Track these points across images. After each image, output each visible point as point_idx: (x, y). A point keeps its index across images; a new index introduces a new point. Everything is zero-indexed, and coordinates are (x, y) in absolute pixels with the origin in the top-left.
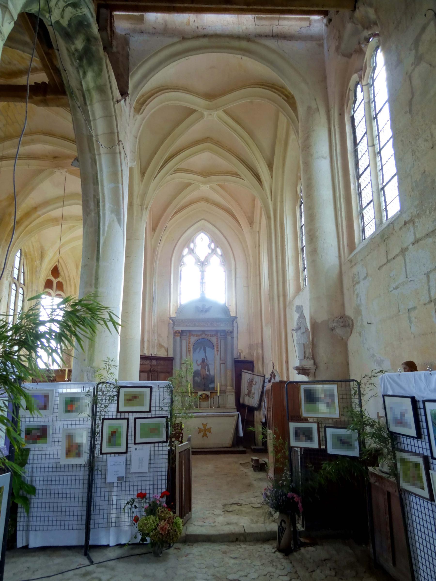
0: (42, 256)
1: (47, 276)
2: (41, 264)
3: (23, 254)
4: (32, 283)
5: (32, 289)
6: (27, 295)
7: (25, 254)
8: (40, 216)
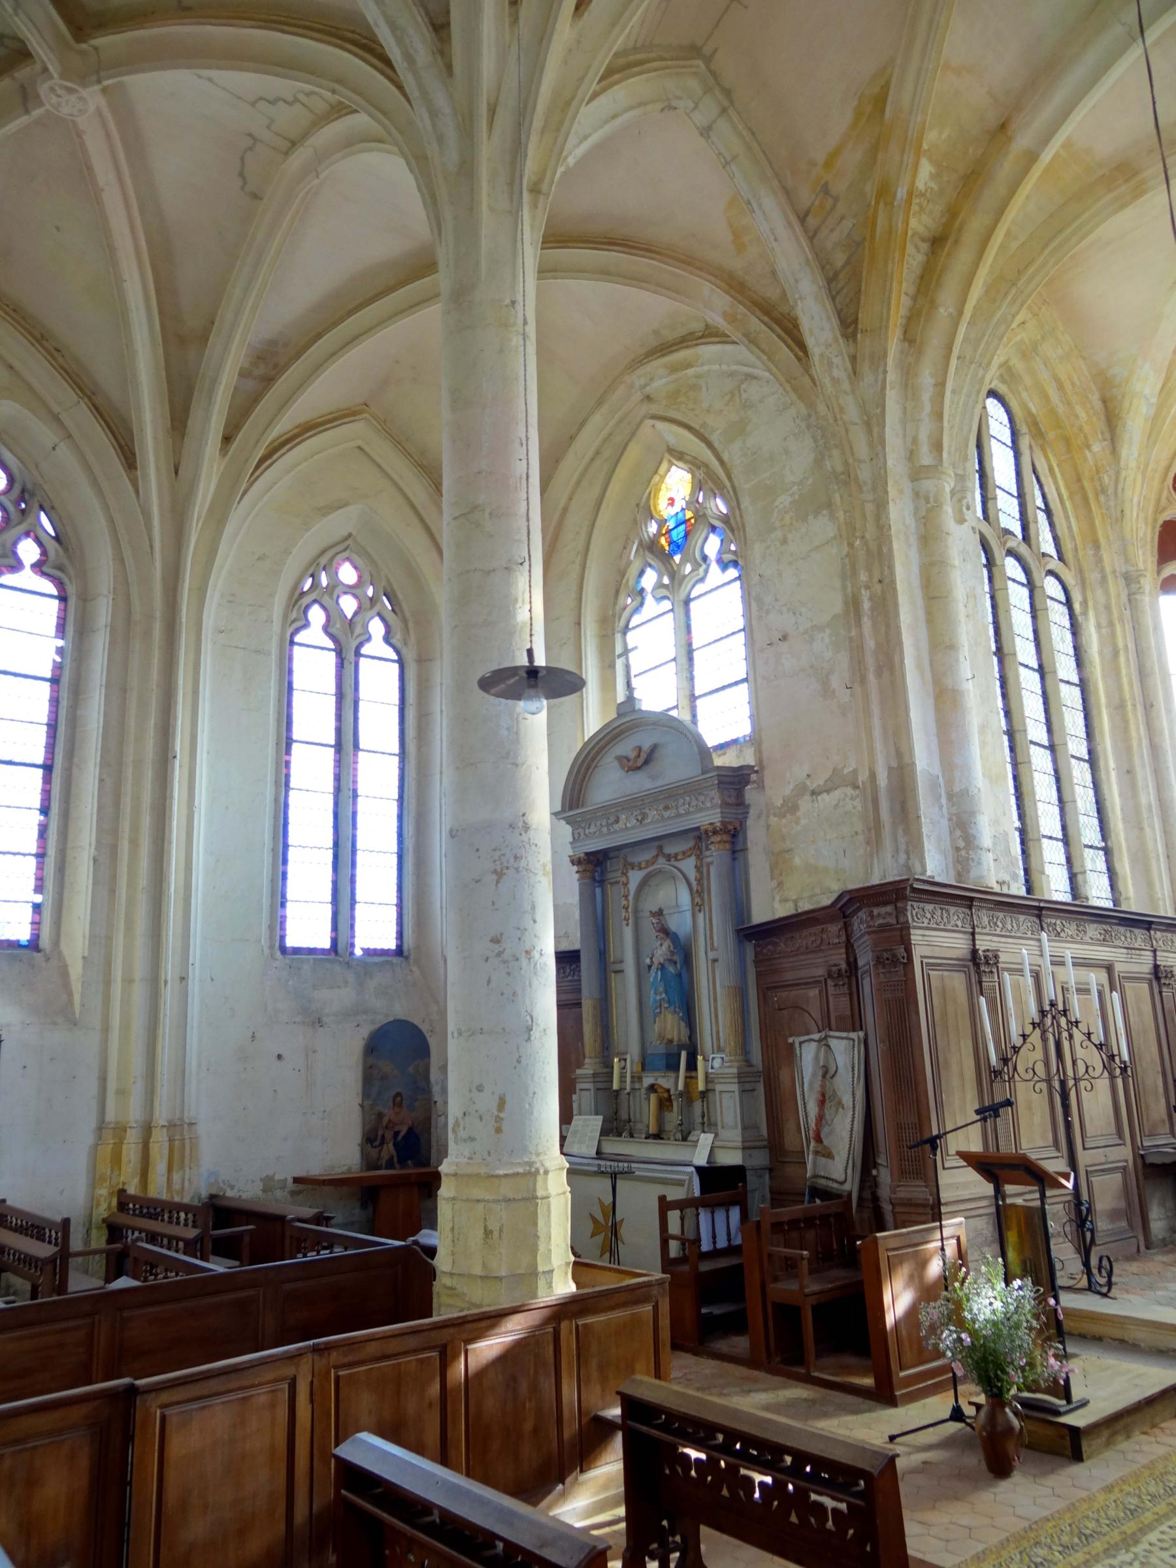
0: (1111, 419)
1: (1158, 510)
2: (1114, 451)
3: (1023, 428)
4: (1096, 545)
5: (1102, 571)
6: (1085, 603)
7: (1034, 424)
8: (1032, 157)
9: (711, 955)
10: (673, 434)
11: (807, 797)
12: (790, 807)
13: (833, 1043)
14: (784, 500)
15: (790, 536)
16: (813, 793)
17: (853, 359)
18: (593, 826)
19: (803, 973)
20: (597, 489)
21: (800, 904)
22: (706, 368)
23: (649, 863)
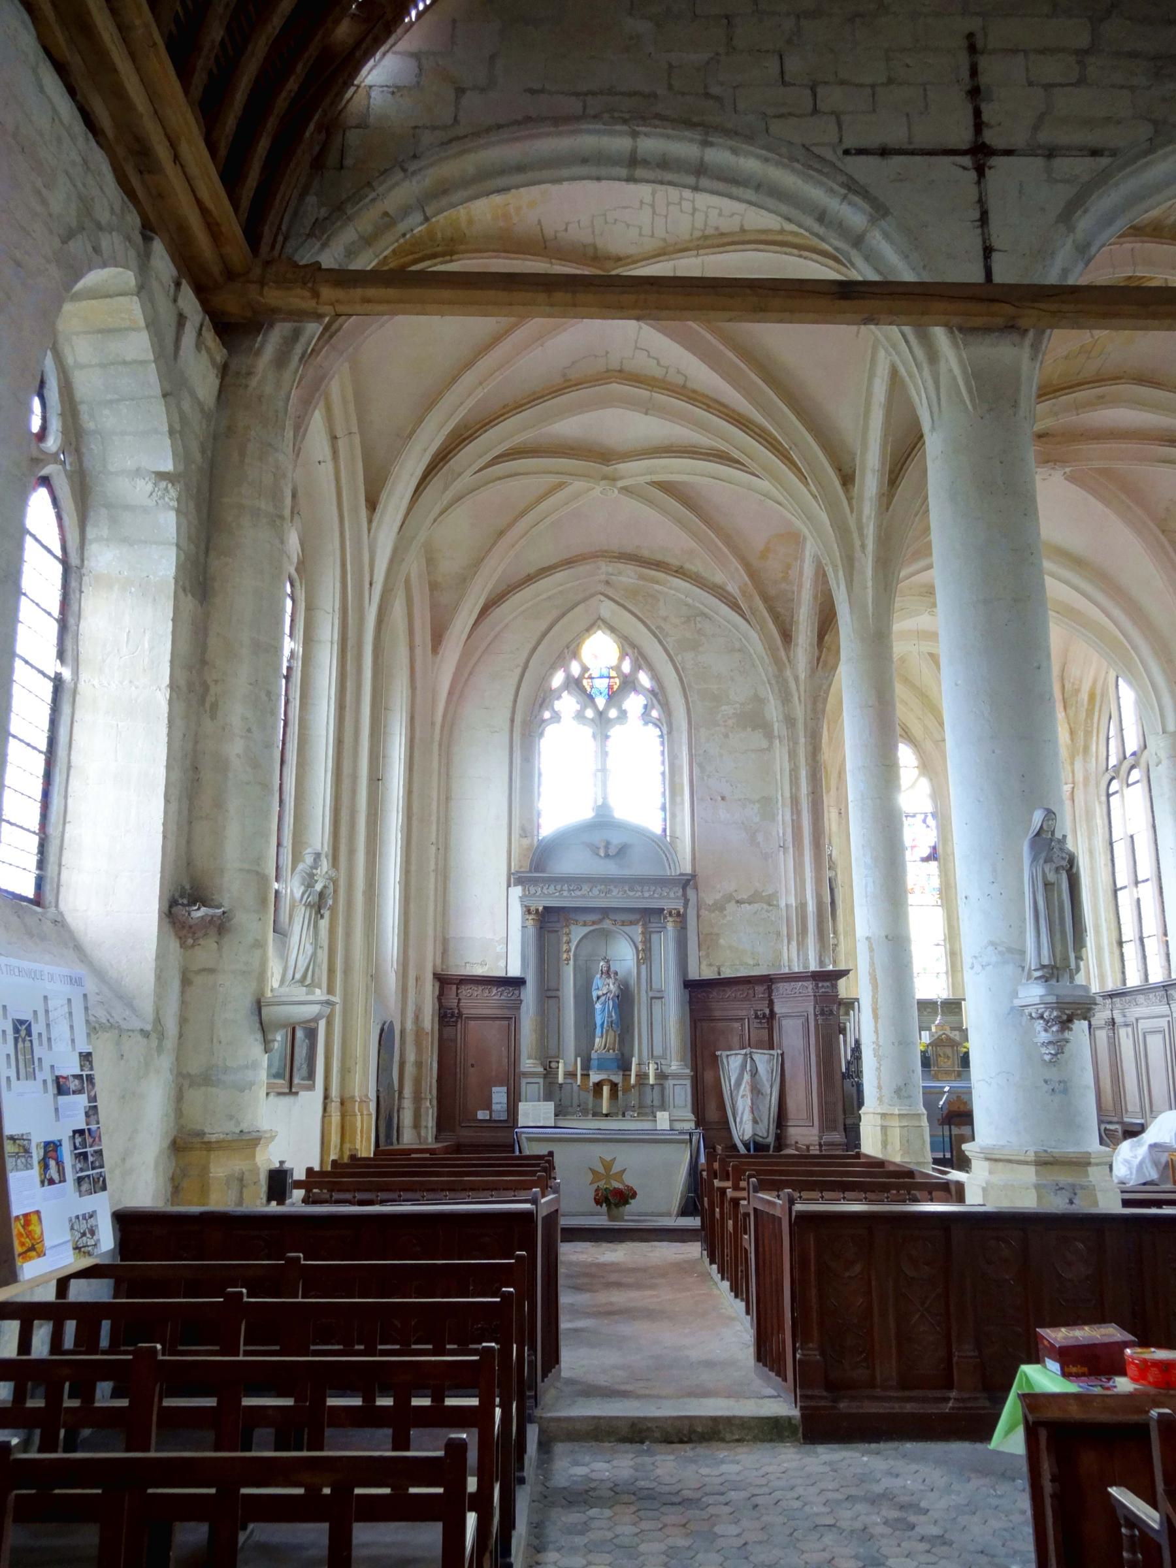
9: (651, 994)
10: (607, 609)
11: (733, 903)
12: (720, 907)
13: (755, 1057)
14: (727, 709)
15: (731, 735)
16: (738, 902)
17: (818, 659)
18: (552, 887)
19: (730, 1013)
20: (544, 626)
21: (723, 969)
22: (673, 592)
23: (594, 923)
